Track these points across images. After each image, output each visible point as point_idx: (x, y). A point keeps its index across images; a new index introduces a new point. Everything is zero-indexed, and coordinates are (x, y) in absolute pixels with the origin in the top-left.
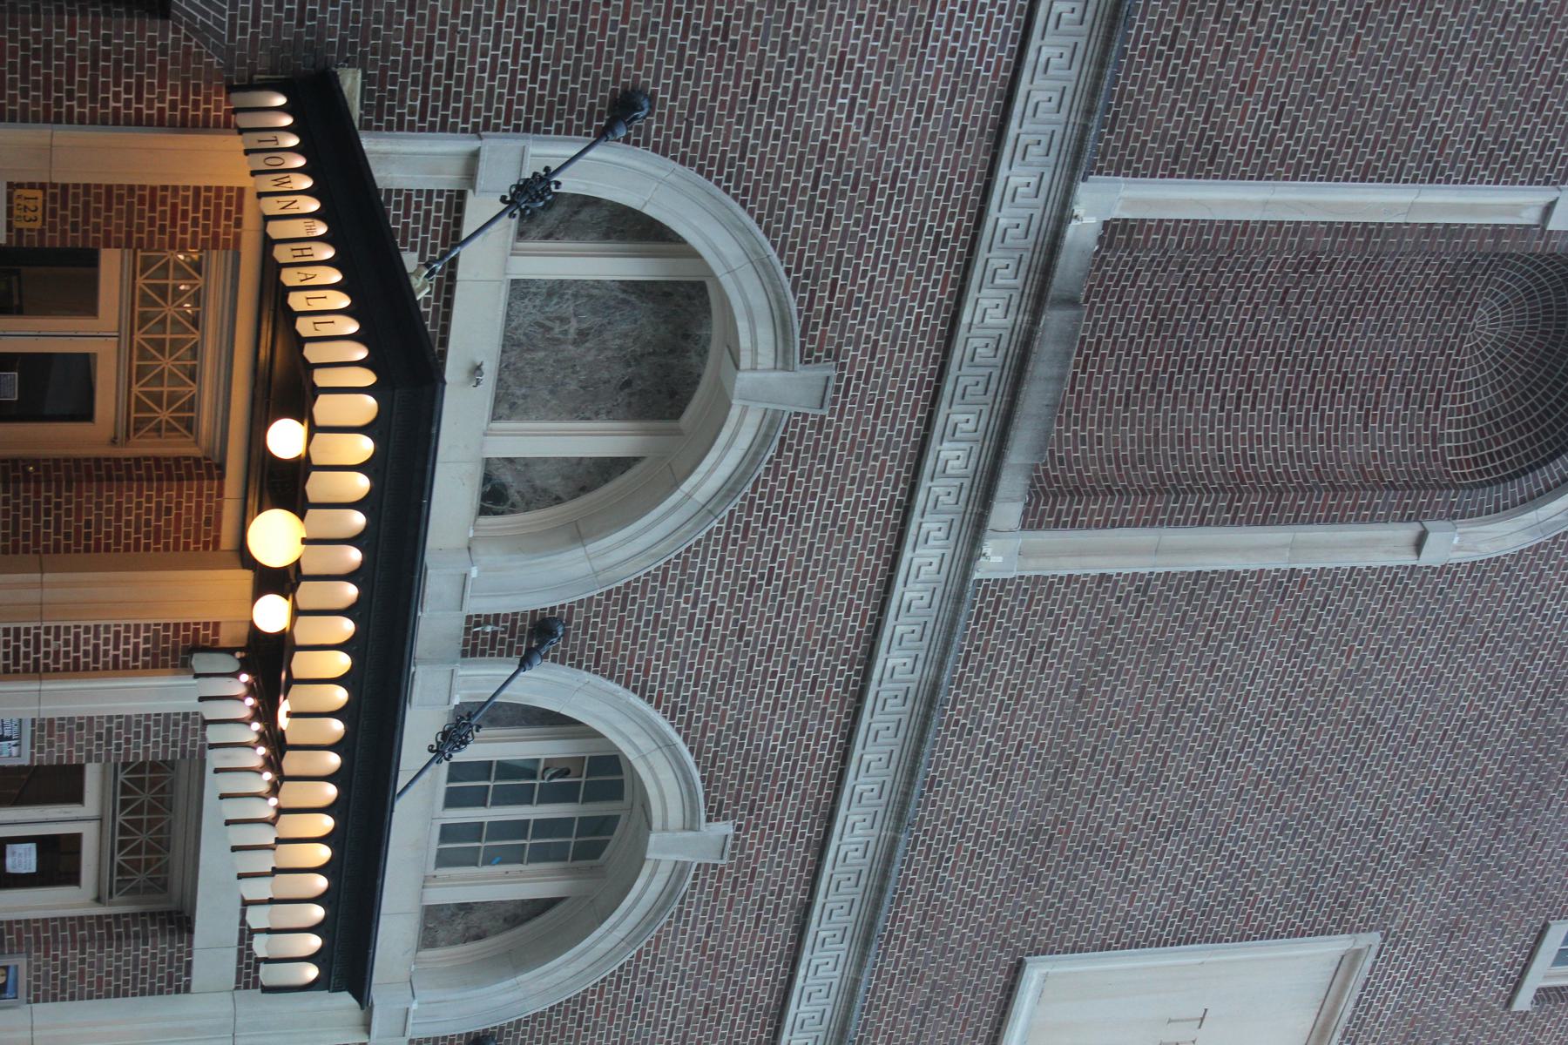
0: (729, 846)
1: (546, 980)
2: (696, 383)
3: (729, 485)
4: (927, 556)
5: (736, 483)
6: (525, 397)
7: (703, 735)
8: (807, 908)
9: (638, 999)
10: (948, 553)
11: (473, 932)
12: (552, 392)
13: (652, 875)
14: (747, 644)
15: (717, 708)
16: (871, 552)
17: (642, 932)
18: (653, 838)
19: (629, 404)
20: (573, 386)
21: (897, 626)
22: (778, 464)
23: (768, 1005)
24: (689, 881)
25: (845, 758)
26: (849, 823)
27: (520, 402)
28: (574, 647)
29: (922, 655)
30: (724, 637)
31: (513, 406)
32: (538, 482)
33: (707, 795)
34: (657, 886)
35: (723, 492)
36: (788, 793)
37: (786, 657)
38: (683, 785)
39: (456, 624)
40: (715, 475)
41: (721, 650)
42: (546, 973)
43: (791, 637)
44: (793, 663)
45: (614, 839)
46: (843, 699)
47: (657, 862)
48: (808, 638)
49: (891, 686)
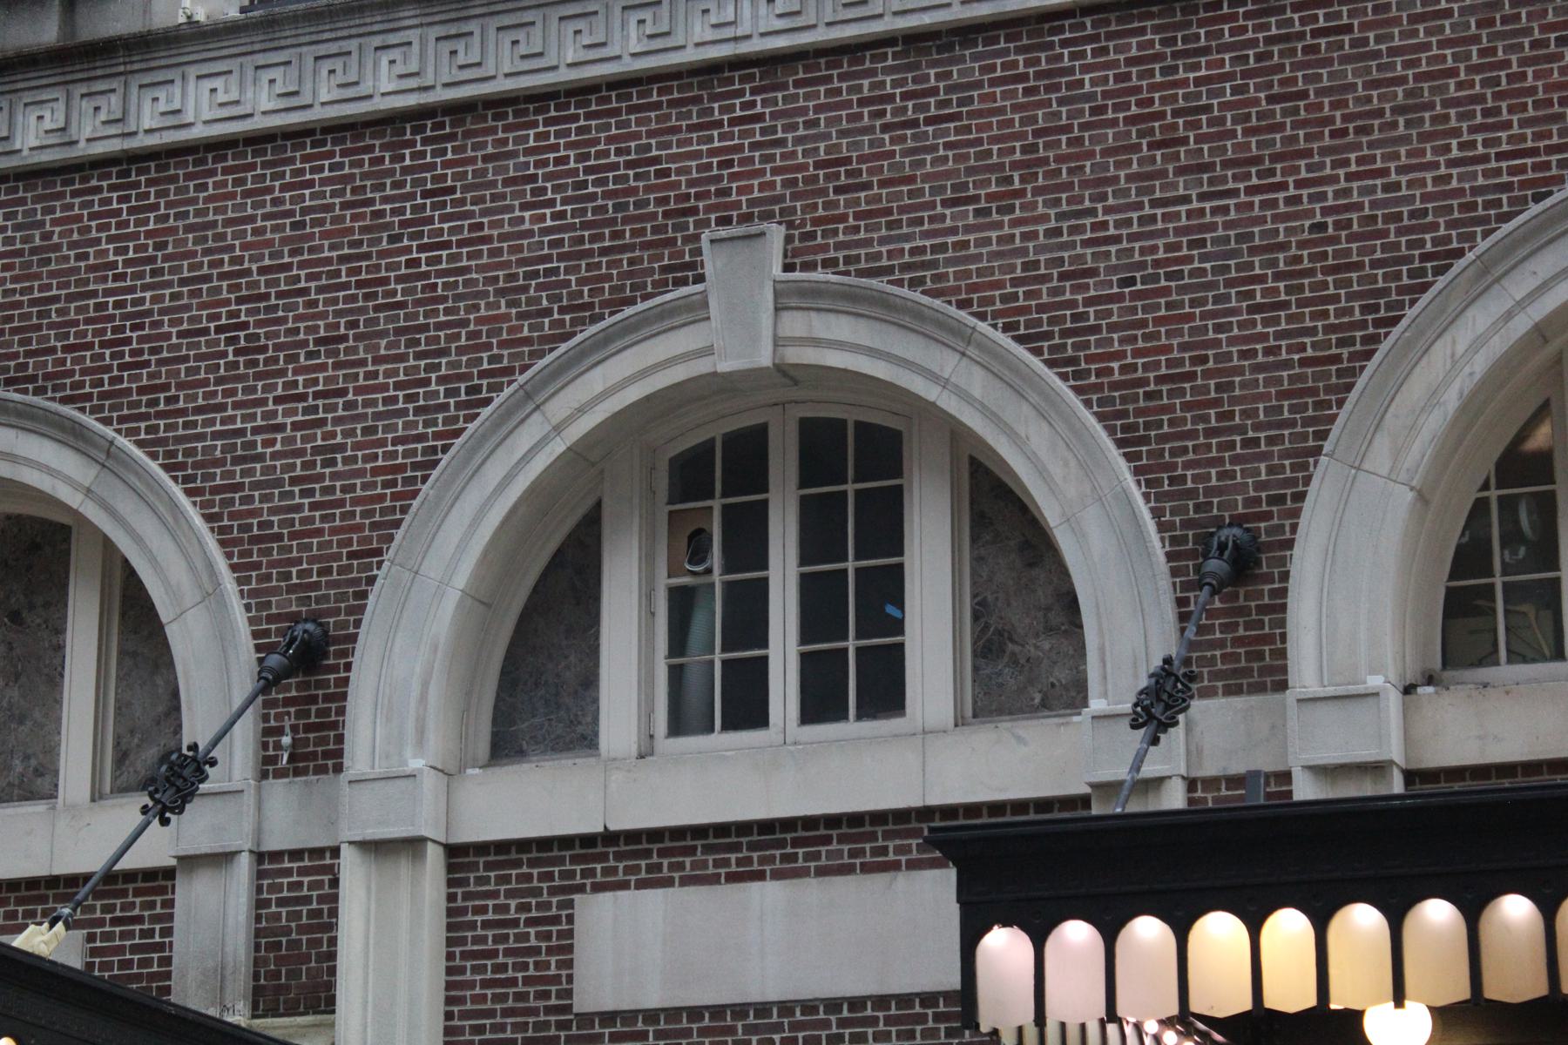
1: (1056, 470)
2: (19, 517)
3: (71, 440)
4: (197, 104)
5: (62, 428)
6: (27, 757)
7: (527, 341)
10: (193, 71)
11: (1056, 618)
12: (21, 720)
13: (816, 342)
14: (353, 325)
15: (473, 335)
16: (204, 187)
17: (940, 325)
18: (724, 367)
19: (47, 605)
20: (14, 693)
21: (325, 97)
22: (47, 377)
24: (819, 275)
25: (582, 92)
26: (710, 35)
27: (33, 762)
28: (341, 597)
29: (377, 41)
30: (337, 366)
31: (38, 773)
32: (160, 709)
33: (645, 297)
34: (841, 327)
35: (81, 445)
36: (656, 160)
37: (382, 254)
38: (612, 348)
39: (280, 792)
40: (54, 464)
41: (363, 363)
42: (1042, 472)
43: (343, 259)
44: (393, 239)
45: (852, 416)
46: (468, 134)
47: (778, 342)
48: (350, 231)
49: (430, 69)
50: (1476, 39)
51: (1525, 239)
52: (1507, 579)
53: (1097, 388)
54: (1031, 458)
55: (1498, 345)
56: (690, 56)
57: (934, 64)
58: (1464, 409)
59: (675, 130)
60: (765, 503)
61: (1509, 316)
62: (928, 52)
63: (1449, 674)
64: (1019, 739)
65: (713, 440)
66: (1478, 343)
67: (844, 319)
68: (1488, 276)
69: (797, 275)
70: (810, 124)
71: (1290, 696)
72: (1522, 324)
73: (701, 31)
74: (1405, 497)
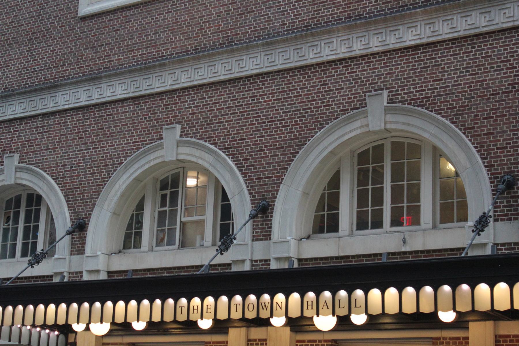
0: (10, 155)
8: (44, 115)
9: (72, 167)
18: (6, 183)
23: (82, 114)
42: (54, 208)
47: (15, 178)
50: (131, 117)
51: (133, 161)
52: (373, 208)
53: (64, 189)
54: (52, 204)
55: (127, 183)
56: (8, 117)
57: (46, 120)
58: (122, 195)
59: (5, 133)
60: (19, 211)
61: (129, 177)
62: (45, 117)
63: (125, 251)
64: (48, 263)
65: (13, 198)
66: (123, 183)
67: (26, 174)
68: (126, 168)
69: (20, 165)
70: (26, 132)
71: (85, 255)
72: (131, 179)
73: (10, 112)
74: (109, 214)
